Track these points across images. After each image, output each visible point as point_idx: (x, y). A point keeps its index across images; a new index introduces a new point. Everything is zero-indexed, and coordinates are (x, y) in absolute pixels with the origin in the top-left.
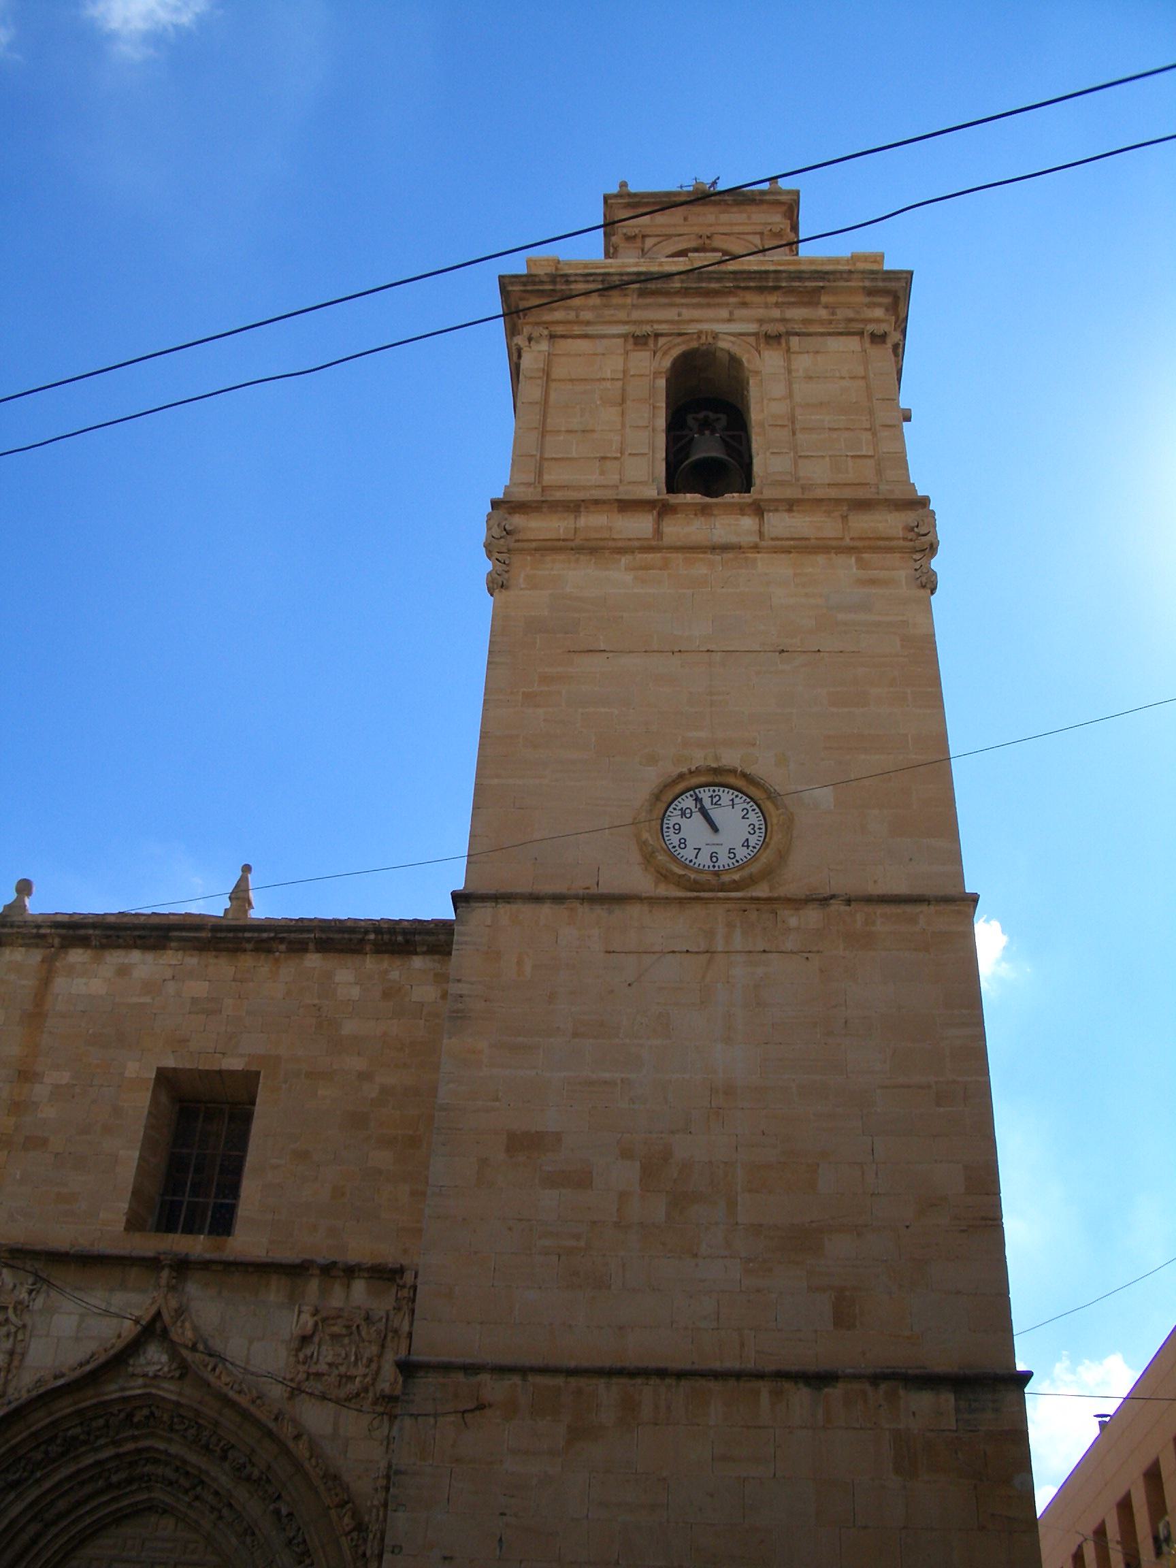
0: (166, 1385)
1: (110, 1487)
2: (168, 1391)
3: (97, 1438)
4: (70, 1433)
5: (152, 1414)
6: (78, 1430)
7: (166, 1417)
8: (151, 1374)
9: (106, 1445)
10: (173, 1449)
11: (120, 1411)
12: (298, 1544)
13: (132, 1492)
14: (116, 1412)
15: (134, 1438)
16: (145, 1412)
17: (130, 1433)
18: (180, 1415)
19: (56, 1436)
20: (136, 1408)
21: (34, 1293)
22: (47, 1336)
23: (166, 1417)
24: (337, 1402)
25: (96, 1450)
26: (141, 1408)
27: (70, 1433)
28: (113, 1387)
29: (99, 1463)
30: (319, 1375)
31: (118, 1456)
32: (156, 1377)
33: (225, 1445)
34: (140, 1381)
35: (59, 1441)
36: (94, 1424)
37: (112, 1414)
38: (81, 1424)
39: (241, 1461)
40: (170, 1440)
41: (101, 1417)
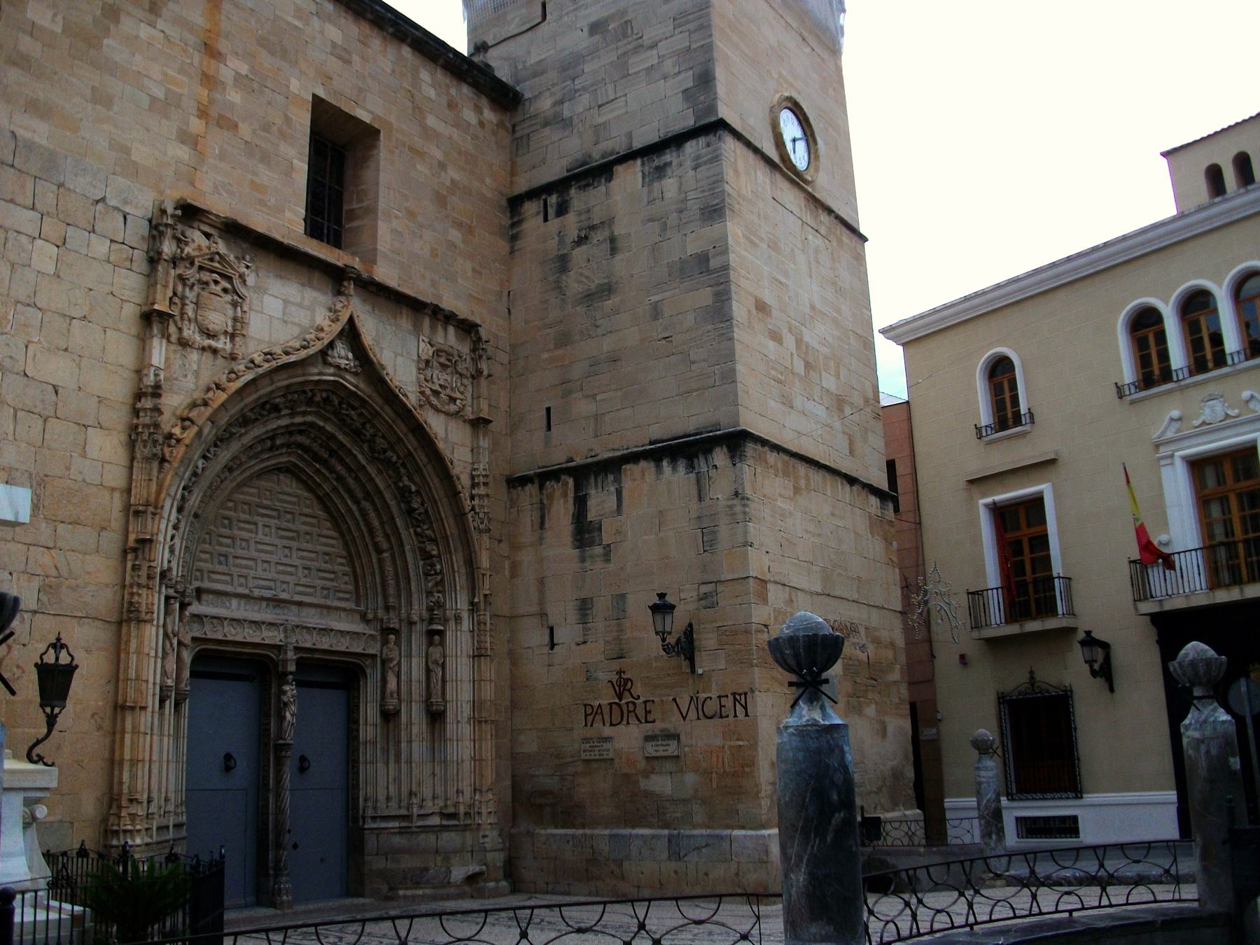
0: (348, 377)
2: (350, 382)
4: (277, 400)
5: (328, 396)
7: (336, 402)
8: (343, 366)
10: (329, 428)
12: (419, 514)
13: (281, 454)
16: (324, 395)
17: (303, 409)
22: (262, 313)
23: (336, 402)
24: (447, 414)
28: (315, 371)
30: (436, 393)
32: (345, 369)
34: (332, 370)
37: (304, 392)
40: (326, 420)
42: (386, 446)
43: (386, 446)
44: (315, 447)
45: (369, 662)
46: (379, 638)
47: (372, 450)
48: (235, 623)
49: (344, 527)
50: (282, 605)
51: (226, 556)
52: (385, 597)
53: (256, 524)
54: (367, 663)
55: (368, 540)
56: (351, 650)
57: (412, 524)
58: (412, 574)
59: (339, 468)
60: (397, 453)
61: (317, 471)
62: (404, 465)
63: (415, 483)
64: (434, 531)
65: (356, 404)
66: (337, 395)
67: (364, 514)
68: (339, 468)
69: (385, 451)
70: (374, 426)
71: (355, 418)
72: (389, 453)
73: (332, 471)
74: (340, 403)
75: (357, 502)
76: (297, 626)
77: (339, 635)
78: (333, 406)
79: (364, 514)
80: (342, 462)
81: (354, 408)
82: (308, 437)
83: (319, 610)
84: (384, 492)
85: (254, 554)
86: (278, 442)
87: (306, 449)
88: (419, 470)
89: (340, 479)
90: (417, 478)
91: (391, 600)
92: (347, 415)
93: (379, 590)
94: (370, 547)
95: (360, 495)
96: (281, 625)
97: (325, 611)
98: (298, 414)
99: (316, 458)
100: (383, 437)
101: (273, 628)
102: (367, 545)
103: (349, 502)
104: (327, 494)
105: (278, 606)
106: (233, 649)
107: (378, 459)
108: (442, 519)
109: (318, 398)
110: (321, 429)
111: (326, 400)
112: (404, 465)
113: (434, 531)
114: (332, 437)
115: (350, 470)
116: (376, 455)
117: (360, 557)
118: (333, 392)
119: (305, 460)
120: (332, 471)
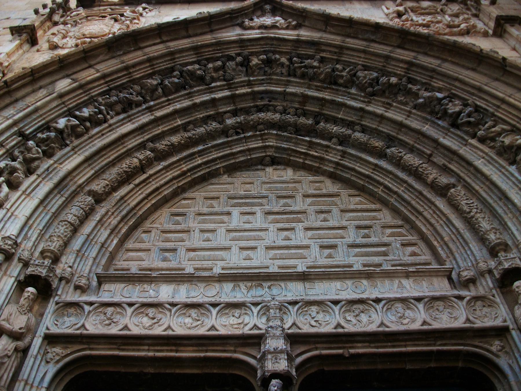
1: (225, 132)
3: (213, 80)
4: (190, 67)
6: (197, 66)
7: (284, 60)
9: (220, 89)
11: (239, 55)
12: (469, 115)
14: (234, 55)
15: (249, 84)
18: (299, 56)
19: (172, 69)
20: (252, 54)
21: (147, 10)
25: (211, 90)
26: (256, 54)
27: (190, 67)
29: (214, 101)
31: (232, 98)
33: (350, 71)
35: (176, 73)
36: (210, 65)
37: (231, 58)
38: (198, 62)
39: (371, 77)
41: (217, 59)
42: (375, 74)
43: (375, 74)
44: (290, 118)
45: (496, 345)
46: (498, 300)
47: (361, 88)
48: (151, 311)
49: (379, 190)
50: (266, 284)
51: (174, 250)
52: (482, 240)
53: (229, 214)
54: (494, 349)
55: (417, 186)
56: (436, 325)
57: (467, 133)
58: (504, 185)
59: (335, 129)
60: (395, 75)
61: (311, 145)
62: (410, 81)
63: (440, 90)
64: (505, 122)
65: (310, 52)
66: (281, 53)
67: (398, 163)
68: (335, 129)
69: (377, 79)
70: (347, 64)
71: (316, 64)
72: (383, 79)
73: (329, 137)
74: (290, 60)
75: (381, 155)
76: (294, 303)
77: (399, 306)
78: (282, 65)
79: (398, 163)
80: (335, 121)
81: (312, 57)
82: (275, 111)
83: (349, 283)
84: (408, 122)
85: (227, 243)
86: (229, 122)
87: (280, 126)
88: (433, 72)
89: (343, 140)
90: (440, 84)
91: (492, 236)
92: (305, 67)
93: (468, 235)
94: (425, 193)
95: (378, 143)
96: (256, 304)
97: (365, 282)
98: (242, 85)
99: (298, 130)
100: (366, 68)
101: (237, 312)
102: (421, 193)
103: (371, 160)
104: (337, 164)
105: (261, 286)
106: (151, 354)
107: (373, 94)
108: (503, 101)
109: (255, 61)
110: (284, 94)
111: (268, 62)
112: (410, 81)
113: (505, 122)
114: (305, 98)
115: (350, 125)
116: (370, 89)
117: (420, 213)
118: (274, 53)
119: (288, 140)
120: (329, 137)
